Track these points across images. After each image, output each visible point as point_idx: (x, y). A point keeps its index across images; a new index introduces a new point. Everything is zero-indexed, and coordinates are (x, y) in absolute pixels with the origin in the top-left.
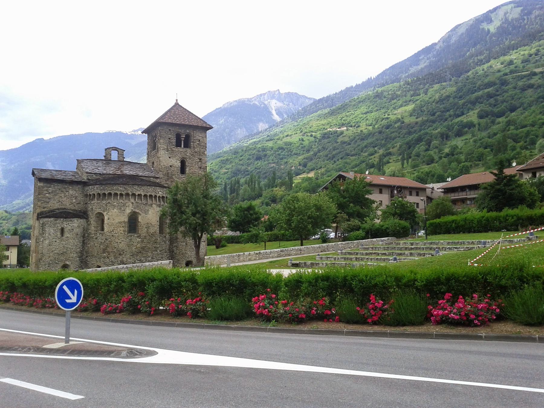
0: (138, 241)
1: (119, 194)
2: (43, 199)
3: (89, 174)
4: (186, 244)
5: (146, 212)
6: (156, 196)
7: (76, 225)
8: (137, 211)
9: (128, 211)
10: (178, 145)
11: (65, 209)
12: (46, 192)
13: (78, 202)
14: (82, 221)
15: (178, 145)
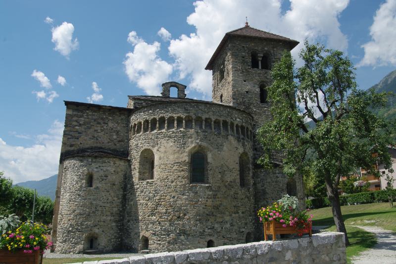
0: (209, 195)
1: (176, 118)
2: (71, 133)
3: (137, 101)
5: (219, 147)
6: (232, 124)
7: (112, 170)
8: (204, 144)
9: (191, 145)
10: (255, 65)
11: (102, 148)
12: (75, 123)
13: (120, 139)
14: (122, 164)
15: (255, 65)
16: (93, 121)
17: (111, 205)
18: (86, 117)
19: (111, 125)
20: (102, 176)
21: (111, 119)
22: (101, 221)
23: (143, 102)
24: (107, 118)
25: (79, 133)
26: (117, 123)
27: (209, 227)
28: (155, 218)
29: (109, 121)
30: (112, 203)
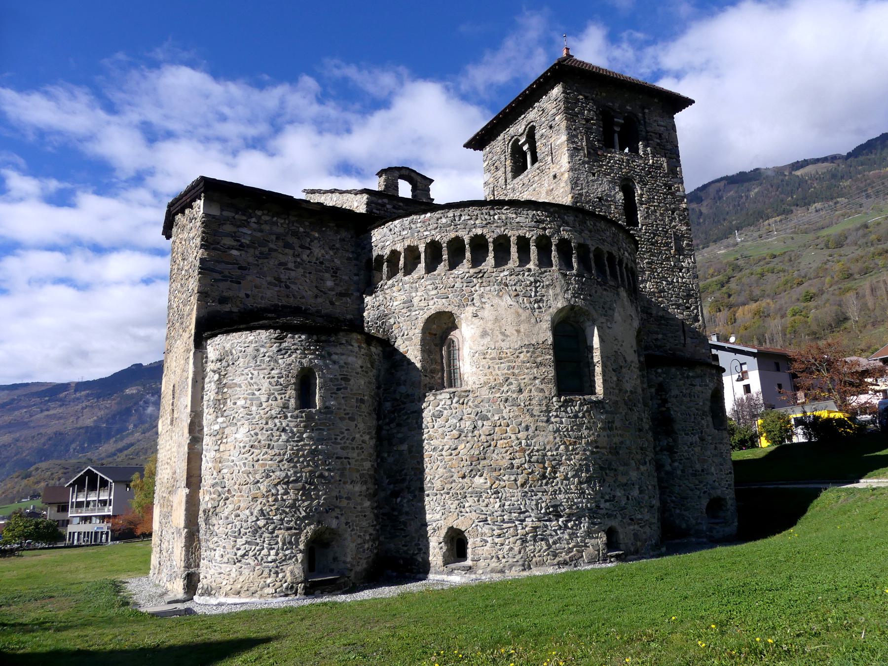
2: (219, 267)
4: (702, 439)
12: (228, 241)
16: (274, 237)
17: (358, 455)
18: (255, 226)
19: (318, 251)
20: (337, 379)
21: (315, 238)
22: (341, 497)
23: (386, 201)
24: (307, 235)
25: (241, 268)
26: (332, 248)
27: (607, 497)
28: (482, 480)
29: (312, 241)
30: (362, 448)
